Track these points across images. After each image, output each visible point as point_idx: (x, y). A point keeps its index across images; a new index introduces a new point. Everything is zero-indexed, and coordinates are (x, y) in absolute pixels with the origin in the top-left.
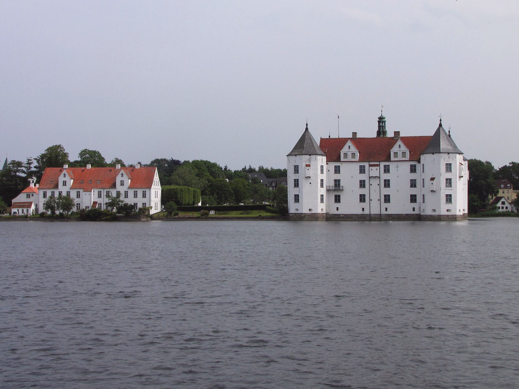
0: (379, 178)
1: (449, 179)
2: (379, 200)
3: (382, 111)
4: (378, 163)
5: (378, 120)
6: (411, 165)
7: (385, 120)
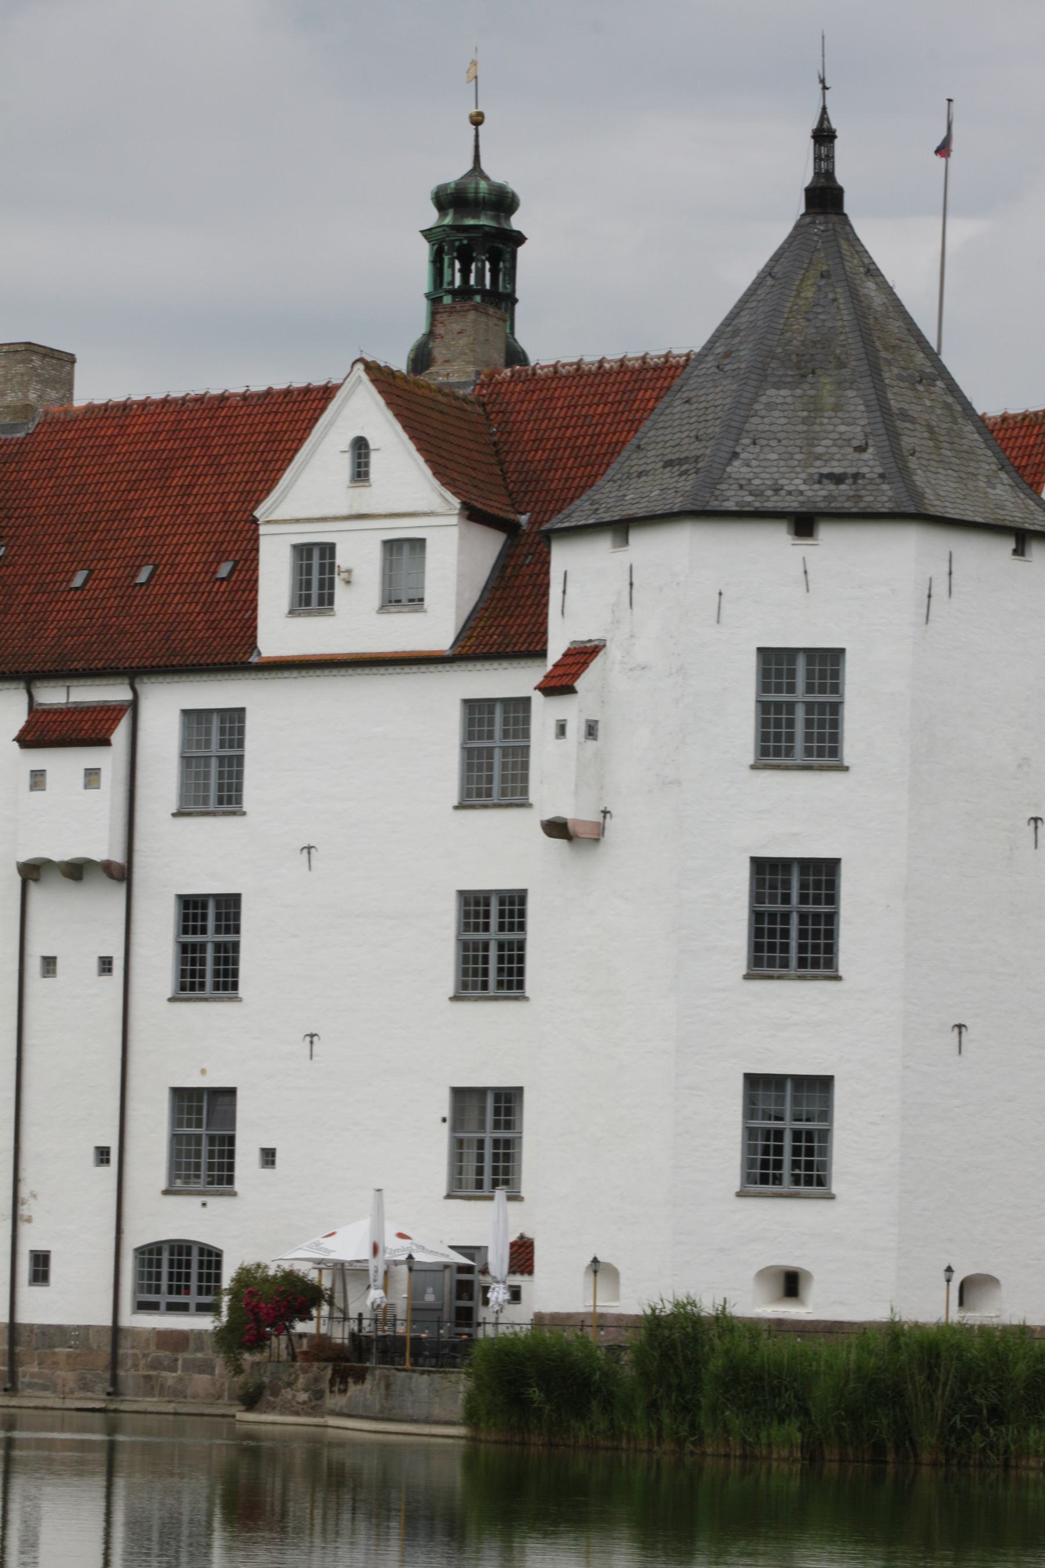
0: (120, 879)
1: (808, 865)
2: (102, 1155)
3: (477, 120)
4: (116, 693)
5: (431, 217)
6: (471, 705)
7: (517, 222)
